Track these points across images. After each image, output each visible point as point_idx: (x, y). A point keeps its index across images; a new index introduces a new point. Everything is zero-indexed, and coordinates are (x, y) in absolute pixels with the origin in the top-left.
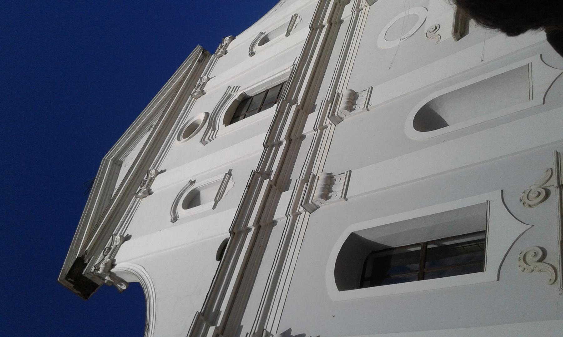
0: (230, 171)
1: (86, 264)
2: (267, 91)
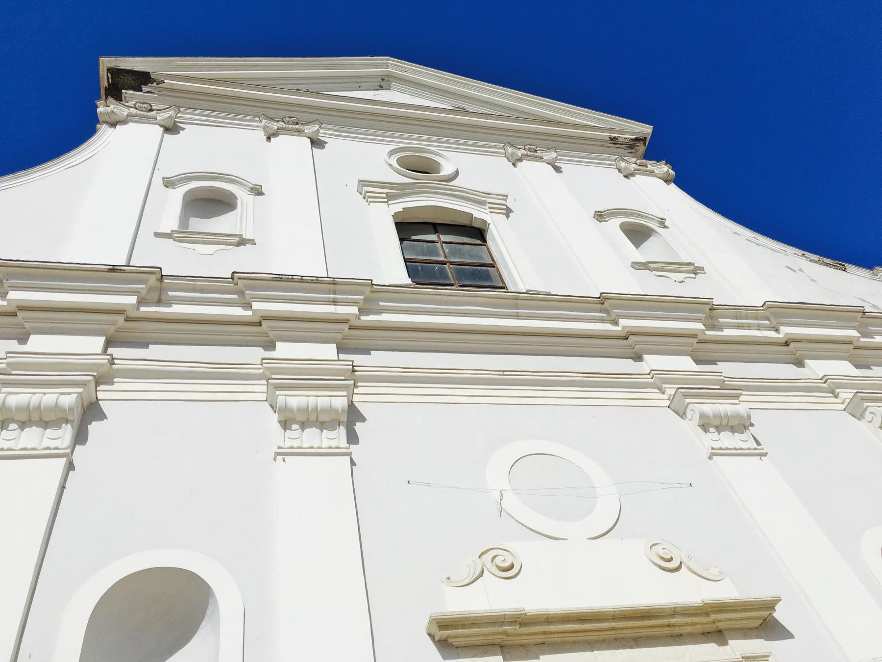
0: (252, 242)
1: (141, 91)
2: (493, 266)
